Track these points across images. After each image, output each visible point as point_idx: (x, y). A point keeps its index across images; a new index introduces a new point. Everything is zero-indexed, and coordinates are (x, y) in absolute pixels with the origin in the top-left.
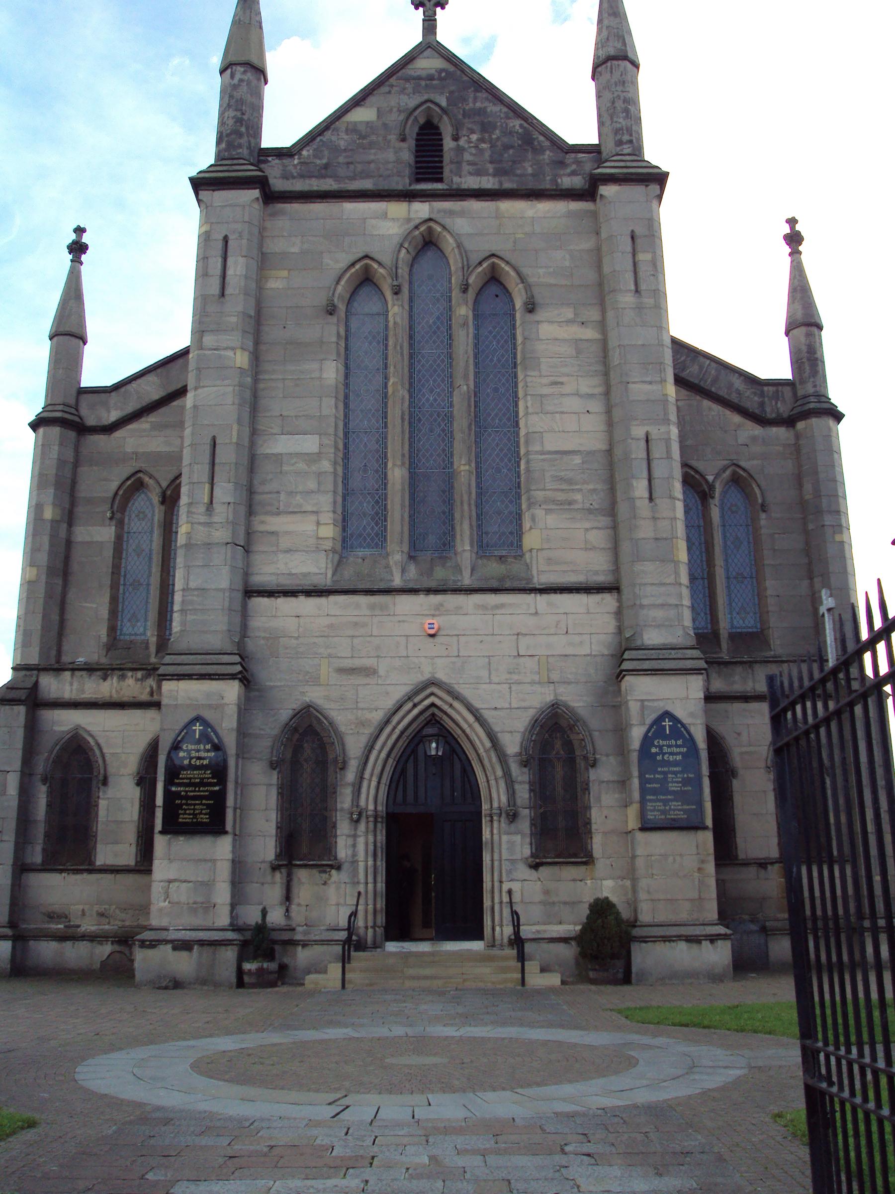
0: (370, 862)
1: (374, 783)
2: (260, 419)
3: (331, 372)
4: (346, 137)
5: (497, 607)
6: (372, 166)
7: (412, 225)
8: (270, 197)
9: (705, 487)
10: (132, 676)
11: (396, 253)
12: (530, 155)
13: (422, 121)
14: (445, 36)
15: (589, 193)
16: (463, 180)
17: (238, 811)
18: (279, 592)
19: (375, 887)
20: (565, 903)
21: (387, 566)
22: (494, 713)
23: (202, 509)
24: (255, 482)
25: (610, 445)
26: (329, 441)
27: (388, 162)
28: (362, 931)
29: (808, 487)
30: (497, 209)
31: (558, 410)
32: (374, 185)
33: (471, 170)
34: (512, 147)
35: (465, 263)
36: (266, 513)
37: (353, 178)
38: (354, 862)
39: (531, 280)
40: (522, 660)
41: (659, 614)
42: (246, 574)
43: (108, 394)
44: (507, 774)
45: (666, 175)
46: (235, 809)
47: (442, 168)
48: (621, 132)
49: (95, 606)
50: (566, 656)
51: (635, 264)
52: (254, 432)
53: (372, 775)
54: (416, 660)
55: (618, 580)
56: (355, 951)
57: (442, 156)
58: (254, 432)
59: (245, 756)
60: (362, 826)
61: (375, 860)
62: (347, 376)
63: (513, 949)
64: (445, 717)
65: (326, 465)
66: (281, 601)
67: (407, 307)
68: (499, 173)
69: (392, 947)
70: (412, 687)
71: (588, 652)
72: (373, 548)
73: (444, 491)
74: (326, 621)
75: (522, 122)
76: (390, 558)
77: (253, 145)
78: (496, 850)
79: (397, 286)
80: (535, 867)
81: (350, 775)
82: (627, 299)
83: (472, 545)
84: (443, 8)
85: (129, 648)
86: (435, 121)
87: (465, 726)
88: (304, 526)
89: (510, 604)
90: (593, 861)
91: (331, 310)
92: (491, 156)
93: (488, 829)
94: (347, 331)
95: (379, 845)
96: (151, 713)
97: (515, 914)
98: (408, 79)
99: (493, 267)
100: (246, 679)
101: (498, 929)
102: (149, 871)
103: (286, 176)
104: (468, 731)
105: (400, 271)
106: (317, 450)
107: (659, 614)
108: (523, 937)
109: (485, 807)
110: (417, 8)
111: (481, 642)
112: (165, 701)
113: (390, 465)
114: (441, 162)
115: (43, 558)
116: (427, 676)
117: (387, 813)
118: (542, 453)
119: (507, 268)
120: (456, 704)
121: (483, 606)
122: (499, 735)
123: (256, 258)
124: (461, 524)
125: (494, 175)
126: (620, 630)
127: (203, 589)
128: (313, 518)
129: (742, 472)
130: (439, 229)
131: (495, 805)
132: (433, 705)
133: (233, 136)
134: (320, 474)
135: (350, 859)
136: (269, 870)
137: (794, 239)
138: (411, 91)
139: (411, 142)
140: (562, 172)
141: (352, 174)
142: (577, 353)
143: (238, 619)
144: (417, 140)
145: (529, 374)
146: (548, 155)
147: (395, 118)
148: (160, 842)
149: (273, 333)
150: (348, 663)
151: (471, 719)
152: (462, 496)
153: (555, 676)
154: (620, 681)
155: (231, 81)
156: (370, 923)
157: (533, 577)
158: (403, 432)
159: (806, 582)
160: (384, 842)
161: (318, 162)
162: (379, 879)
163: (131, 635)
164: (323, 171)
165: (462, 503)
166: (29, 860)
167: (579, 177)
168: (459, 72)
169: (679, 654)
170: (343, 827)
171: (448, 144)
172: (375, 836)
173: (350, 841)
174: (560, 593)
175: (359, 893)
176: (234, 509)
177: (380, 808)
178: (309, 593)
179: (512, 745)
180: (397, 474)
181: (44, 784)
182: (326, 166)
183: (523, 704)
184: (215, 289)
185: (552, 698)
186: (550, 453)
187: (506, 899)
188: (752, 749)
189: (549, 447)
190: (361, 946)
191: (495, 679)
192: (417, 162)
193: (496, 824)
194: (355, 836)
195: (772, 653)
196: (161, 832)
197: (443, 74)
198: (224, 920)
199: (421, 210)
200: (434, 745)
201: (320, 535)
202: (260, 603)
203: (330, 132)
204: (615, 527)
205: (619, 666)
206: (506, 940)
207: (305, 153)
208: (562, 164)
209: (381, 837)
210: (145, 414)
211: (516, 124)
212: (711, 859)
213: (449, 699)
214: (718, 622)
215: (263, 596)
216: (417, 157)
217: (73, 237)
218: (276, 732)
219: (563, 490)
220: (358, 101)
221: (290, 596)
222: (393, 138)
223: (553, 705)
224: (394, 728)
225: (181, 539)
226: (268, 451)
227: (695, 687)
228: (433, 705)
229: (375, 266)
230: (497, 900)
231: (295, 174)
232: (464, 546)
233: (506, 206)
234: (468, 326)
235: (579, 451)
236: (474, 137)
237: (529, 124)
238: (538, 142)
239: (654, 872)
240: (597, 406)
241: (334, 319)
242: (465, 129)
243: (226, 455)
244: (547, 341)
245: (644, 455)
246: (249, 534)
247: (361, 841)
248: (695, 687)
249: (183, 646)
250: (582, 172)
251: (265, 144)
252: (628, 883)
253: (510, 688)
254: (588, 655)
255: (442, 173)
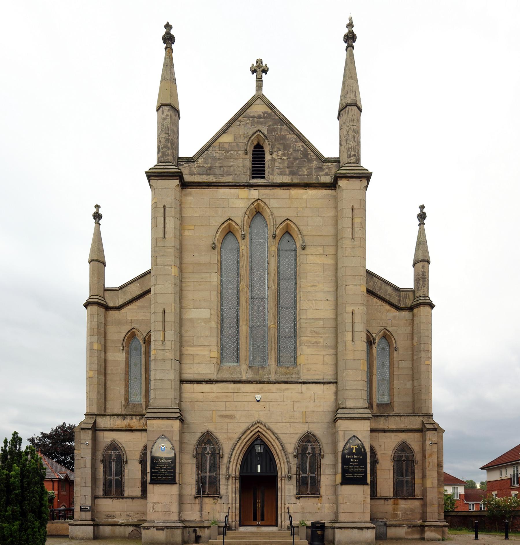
0: (234, 496)
1: (235, 464)
2: (183, 301)
3: (215, 279)
4: (219, 152)
5: (286, 389)
6: (232, 168)
7: (250, 203)
8: (184, 185)
9: (372, 339)
10: (135, 418)
11: (243, 217)
12: (306, 164)
13: (255, 143)
14: (266, 92)
15: (333, 186)
16: (274, 177)
17: (181, 474)
18: (194, 382)
19: (235, 505)
20: (310, 513)
21: (240, 371)
22: (284, 435)
23: (161, 343)
24: (183, 331)
25: (336, 316)
26: (214, 312)
27: (239, 167)
28: (230, 523)
29: (416, 339)
30: (290, 194)
31: (314, 299)
32: (233, 179)
33: (278, 172)
34: (298, 159)
35: (275, 223)
36: (188, 346)
37: (223, 176)
38: (227, 495)
39: (304, 233)
40: (295, 413)
41: (352, 393)
42: (181, 374)
43: (117, 291)
44: (288, 461)
45: (370, 174)
46: (179, 473)
47: (264, 171)
48: (350, 150)
49: (118, 388)
50: (313, 411)
51: (353, 224)
52: (181, 308)
53: (234, 460)
54: (252, 412)
55: (337, 379)
56: (228, 530)
57: (264, 164)
58: (181, 308)
59: (183, 452)
60: (230, 480)
61: (235, 495)
62: (221, 280)
63: (289, 530)
64: (263, 437)
65: (213, 324)
66: (196, 386)
67: (248, 246)
68: (292, 173)
69: (242, 529)
70: (250, 424)
71: (323, 410)
72: (233, 363)
73: (264, 337)
74: (214, 395)
75: (303, 144)
76: (241, 367)
77: (175, 155)
78: (283, 491)
79: (244, 235)
80: (298, 498)
81: (225, 460)
82: (348, 242)
83: (275, 362)
84: (266, 74)
85: (134, 407)
86: (261, 144)
87: (271, 440)
88: (205, 352)
89: (291, 388)
90: (321, 496)
91: (214, 247)
92: (288, 164)
93: (280, 483)
94: (221, 258)
95: (237, 488)
96: (144, 434)
97: (290, 517)
98: (248, 118)
99: (287, 226)
100: (182, 420)
101: (283, 522)
102: (146, 498)
103: (191, 174)
104: (273, 442)
105: (245, 227)
106: (209, 317)
107: (352, 393)
108: (294, 526)
109: (279, 474)
110: (253, 74)
111: (279, 405)
112: (149, 429)
113: (241, 324)
114: (264, 167)
115: (95, 366)
116: (255, 420)
117: (240, 476)
118: (306, 319)
119: (294, 226)
120: (268, 431)
121: (280, 389)
122: (285, 444)
123: (179, 218)
124: (271, 352)
125: (289, 175)
126: (336, 400)
127: (163, 380)
128: (208, 348)
129: (388, 333)
130: (263, 205)
131: (283, 473)
132: (259, 431)
133: (165, 149)
134: (211, 328)
135: (225, 494)
136: (193, 498)
137: (422, 217)
138: (250, 125)
139: (250, 156)
140: (321, 173)
141: (222, 173)
142: (324, 271)
143: (178, 393)
144: (253, 154)
145: (301, 281)
146: (315, 164)
147: (243, 141)
148: (150, 487)
149: (188, 259)
150: (224, 413)
151: (274, 437)
152: (271, 339)
153: (309, 420)
154: (335, 422)
155: (162, 115)
156: (234, 520)
157: (301, 376)
158: (246, 309)
159: (411, 382)
160: (239, 487)
161: (206, 165)
162: (237, 502)
163: (134, 401)
164: (209, 171)
165: (271, 343)
166: (97, 494)
167: (329, 177)
168: (273, 113)
169: (361, 411)
170: (223, 481)
171: (268, 157)
172: (235, 485)
173: (225, 487)
174: (312, 384)
175: (229, 508)
176: (174, 343)
177: (237, 474)
178: (207, 382)
179: (291, 448)
180: (244, 328)
181: (102, 463)
182: (210, 168)
183: (296, 432)
184: (161, 235)
185: (307, 429)
186: (310, 319)
187: (287, 511)
188: (385, 452)
189: (310, 316)
190: (230, 528)
191: (284, 421)
192: (253, 167)
193: (283, 481)
194: (227, 485)
195: (394, 413)
196: (150, 483)
197: (266, 115)
198: (175, 518)
199: (255, 194)
200: (259, 448)
201: (212, 356)
202: (186, 386)
203: (211, 148)
204: (336, 355)
205: (335, 416)
206: (286, 527)
207: (200, 161)
208: (321, 169)
209: (238, 486)
210: (134, 302)
211: (300, 145)
212: (369, 497)
213: (265, 429)
214: (373, 399)
215: (188, 383)
216: (253, 164)
217: (94, 210)
218: (195, 442)
219: (314, 337)
220: (224, 131)
221: (200, 383)
222: (242, 152)
223: (307, 432)
224: (243, 441)
225: (152, 357)
226: (188, 317)
227: (366, 426)
228: (259, 431)
229: (234, 224)
230: (283, 511)
231: (195, 173)
232: (272, 362)
233: (294, 192)
234: (275, 257)
235: (322, 319)
236: (280, 153)
237: (306, 145)
238: (310, 156)
239: (346, 501)
240: (331, 297)
241: (215, 252)
242: (276, 148)
243: (170, 318)
244: (310, 265)
245: (351, 321)
246: (181, 355)
247: (230, 487)
248: (366, 426)
249: (155, 405)
250: (330, 173)
251: (181, 155)
252: (335, 506)
253: (290, 425)
254: (322, 411)
255: (264, 174)
